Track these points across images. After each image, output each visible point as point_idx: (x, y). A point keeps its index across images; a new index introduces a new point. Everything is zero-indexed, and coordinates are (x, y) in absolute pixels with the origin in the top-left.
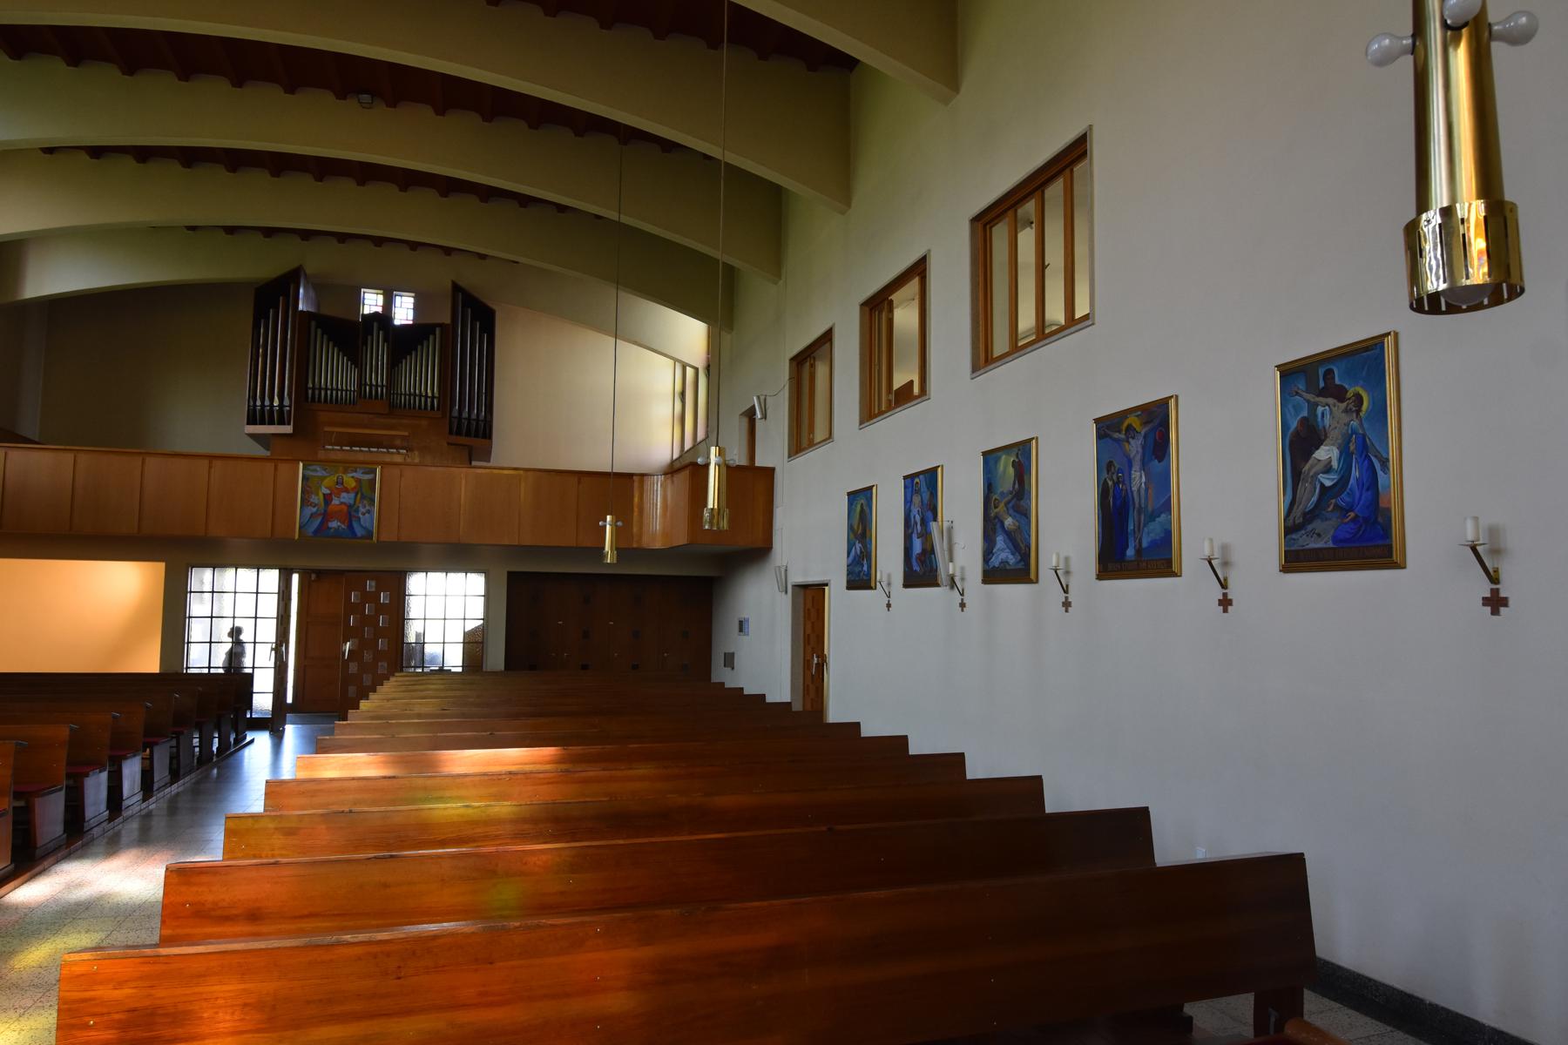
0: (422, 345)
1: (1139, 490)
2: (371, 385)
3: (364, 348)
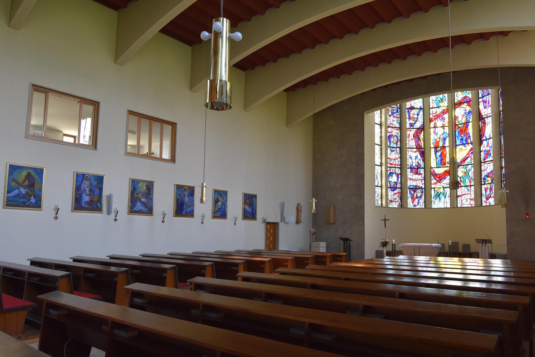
1: (187, 202)
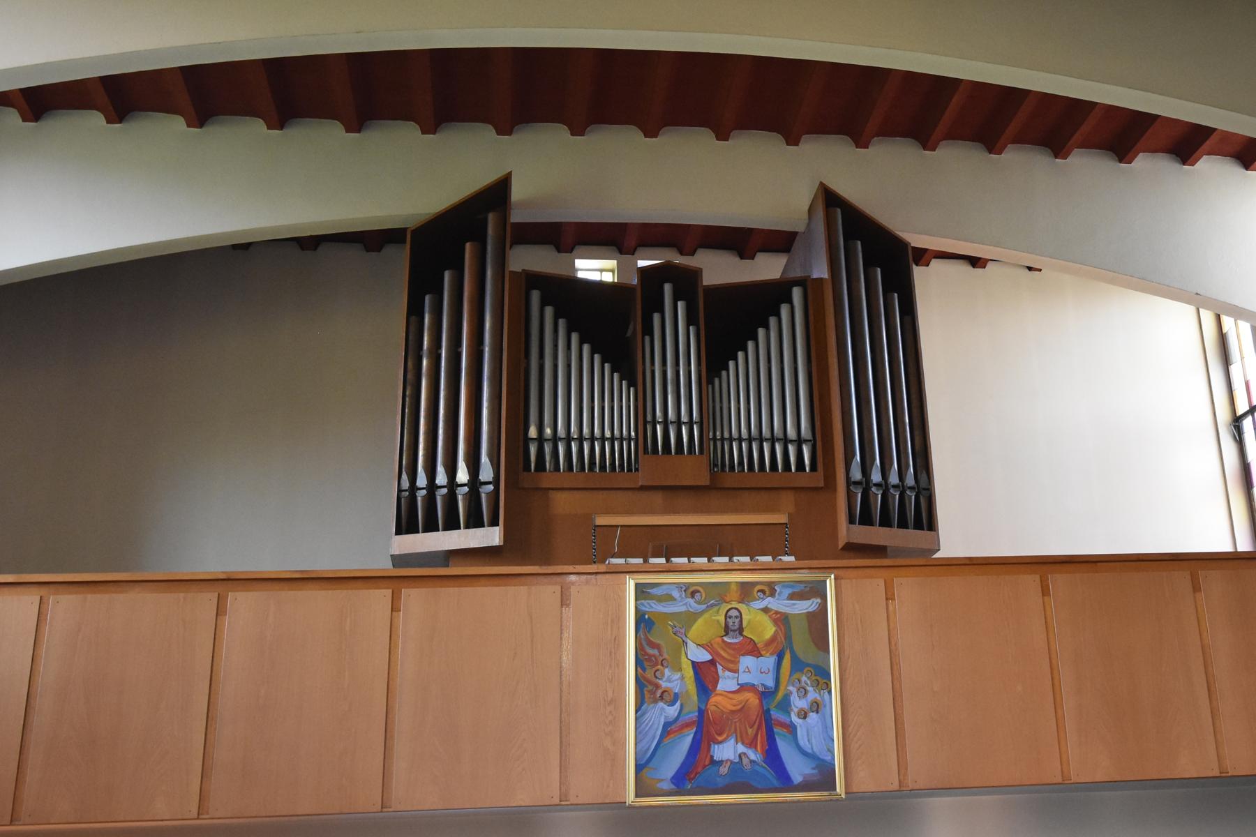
0: (767, 327)
3: (647, 339)
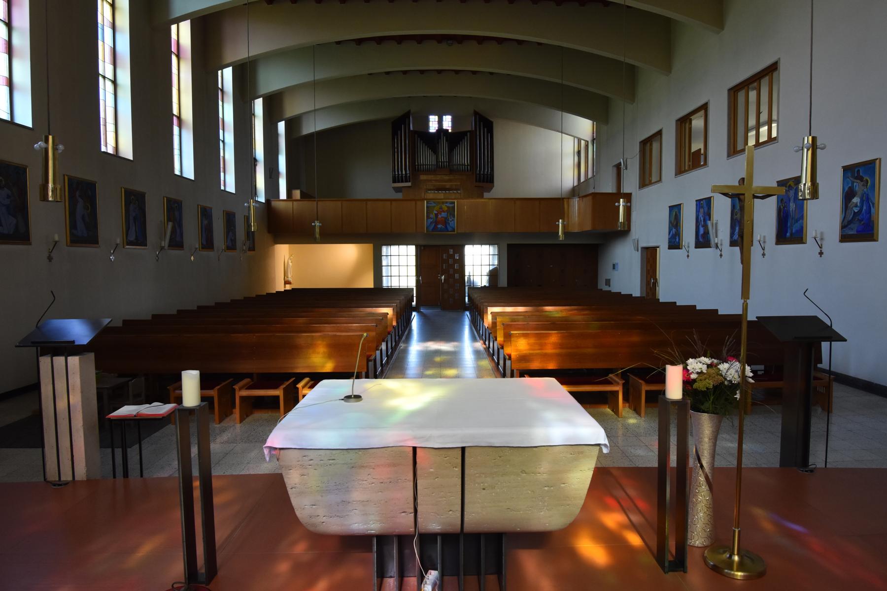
2: (441, 162)
